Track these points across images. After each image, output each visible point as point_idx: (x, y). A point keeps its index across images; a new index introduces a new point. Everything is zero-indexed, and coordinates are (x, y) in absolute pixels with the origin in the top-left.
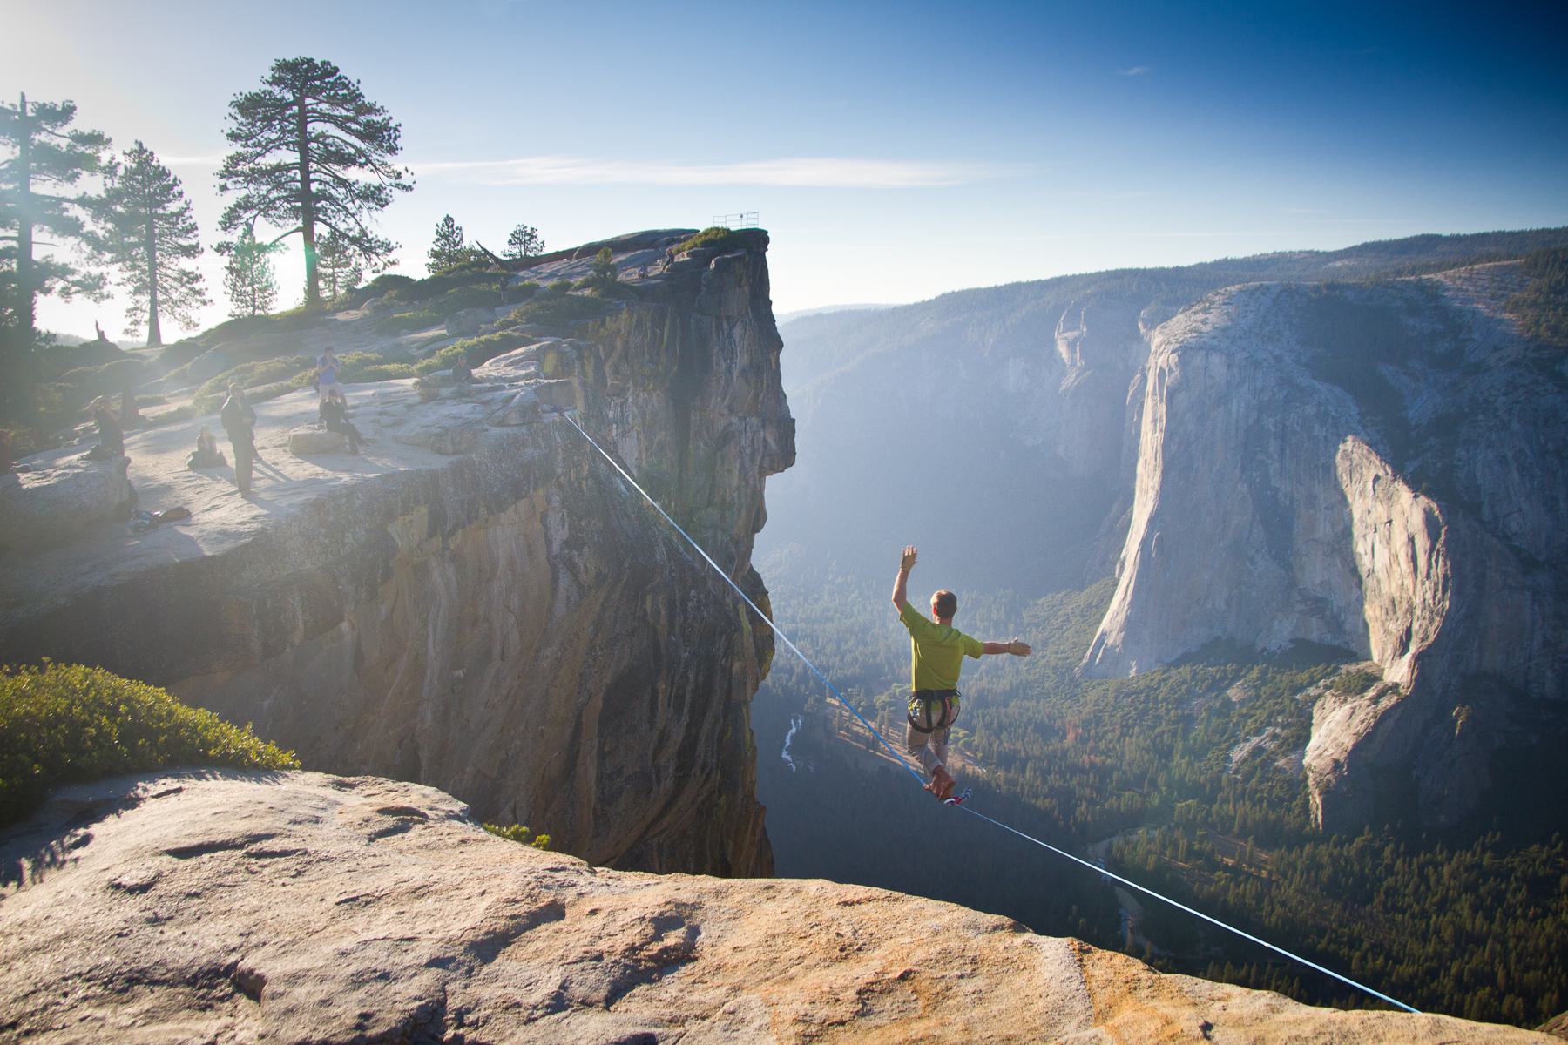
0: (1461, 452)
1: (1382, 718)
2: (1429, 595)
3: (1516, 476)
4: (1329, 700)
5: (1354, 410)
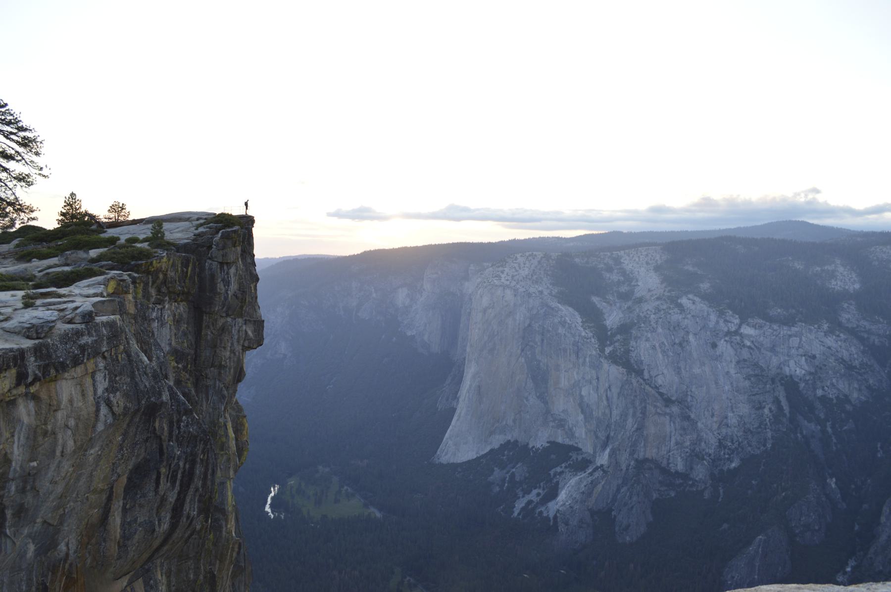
0: (633, 343)
3: (660, 356)
5: (579, 320)
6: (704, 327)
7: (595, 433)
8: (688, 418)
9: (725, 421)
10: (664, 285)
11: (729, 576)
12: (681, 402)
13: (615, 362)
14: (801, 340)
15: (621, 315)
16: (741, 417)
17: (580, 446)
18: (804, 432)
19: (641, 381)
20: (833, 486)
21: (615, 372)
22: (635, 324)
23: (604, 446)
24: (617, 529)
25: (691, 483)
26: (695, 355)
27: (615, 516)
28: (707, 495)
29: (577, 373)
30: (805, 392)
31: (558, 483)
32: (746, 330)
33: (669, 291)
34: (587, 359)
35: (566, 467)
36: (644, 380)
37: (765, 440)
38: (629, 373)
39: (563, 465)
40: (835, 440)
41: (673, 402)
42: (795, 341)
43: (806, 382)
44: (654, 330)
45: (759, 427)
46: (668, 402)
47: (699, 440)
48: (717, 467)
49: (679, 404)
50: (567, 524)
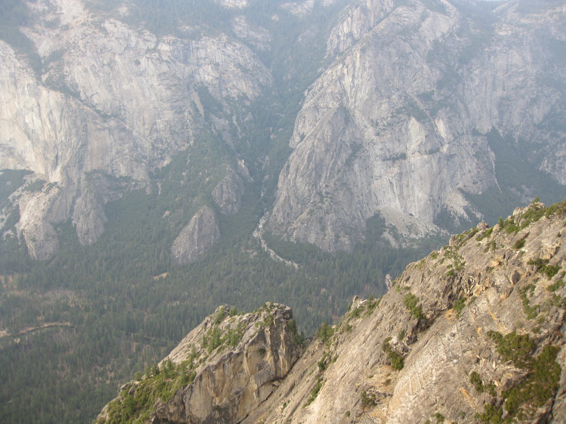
0: (66, 68)
1: (53, 201)
2: (63, 138)
3: (93, 77)
4: (26, 197)
5: (12, 52)
6: (127, 48)
7: (44, 155)
8: (124, 129)
9: (155, 127)
10: (87, 11)
11: (176, 252)
12: (116, 116)
13: (54, 89)
14: (206, 51)
15: (52, 44)
16: (167, 122)
17: (32, 169)
18: (217, 127)
19: (79, 102)
20: (243, 166)
21: (51, 98)
22: (66, 50)
23: (55, 165)
24: (79, 235)
25: (134, 183)
26: (123, 73)
27: (75, 225)
28: (148, 192)
29: (19, 103)
30: (213, 94)
31: (18, 206)
32: (164, 47)
33: (92, 17)
34: (26, 89)
35: (23, 191)
36: (82, 101)
37: (188, 137)
38: (67, 97)
39: (20, 189)
40: (240, 131)
41: (109, 117)
42: (202, 53)
43: (214, 86)
44: (84, 55)
45: (183, 128)
46: (105, 117)
47: (136, 146)
48: (152, 166)
49: (113, 116)
50: (34, 240)
